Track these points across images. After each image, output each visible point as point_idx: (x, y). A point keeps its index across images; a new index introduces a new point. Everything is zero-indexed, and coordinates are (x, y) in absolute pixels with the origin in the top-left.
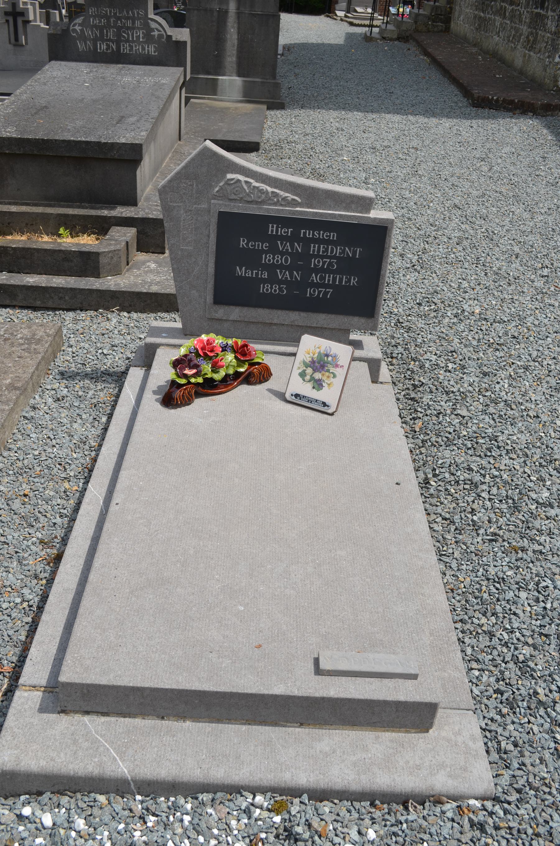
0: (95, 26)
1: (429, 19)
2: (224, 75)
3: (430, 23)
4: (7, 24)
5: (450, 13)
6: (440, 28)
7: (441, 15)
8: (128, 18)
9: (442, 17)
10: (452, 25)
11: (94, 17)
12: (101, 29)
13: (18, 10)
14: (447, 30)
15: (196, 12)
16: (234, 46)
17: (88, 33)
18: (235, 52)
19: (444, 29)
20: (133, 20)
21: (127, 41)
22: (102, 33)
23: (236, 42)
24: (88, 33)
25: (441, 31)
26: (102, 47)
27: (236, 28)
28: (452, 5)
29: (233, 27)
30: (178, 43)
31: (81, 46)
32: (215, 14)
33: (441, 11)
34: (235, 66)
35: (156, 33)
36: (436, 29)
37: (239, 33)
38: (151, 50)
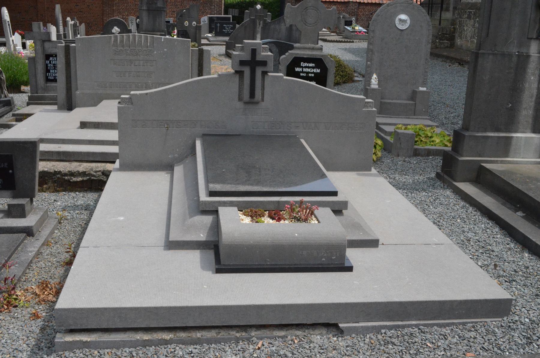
1: (436, 38)
2: (516, 132)
3: (437, 41)
4: (238, 76)
5: (454, 32)
6: (446, 45)
7: (447, 34)
9: (448, 36)
10: (458, 42)
13: (258, 58)
14: (452, 45)
15: (491, 57)
16: (532, 97)
18: (532, 104)
19: (449, 45)
23: (535, 92)
25: (447, 47)
27: (537, 76)
28: (455, 26)
29: (533, 74)
32: (515, 59)
33: (447, 31)
34: (530, 120)
36: (442, 46)
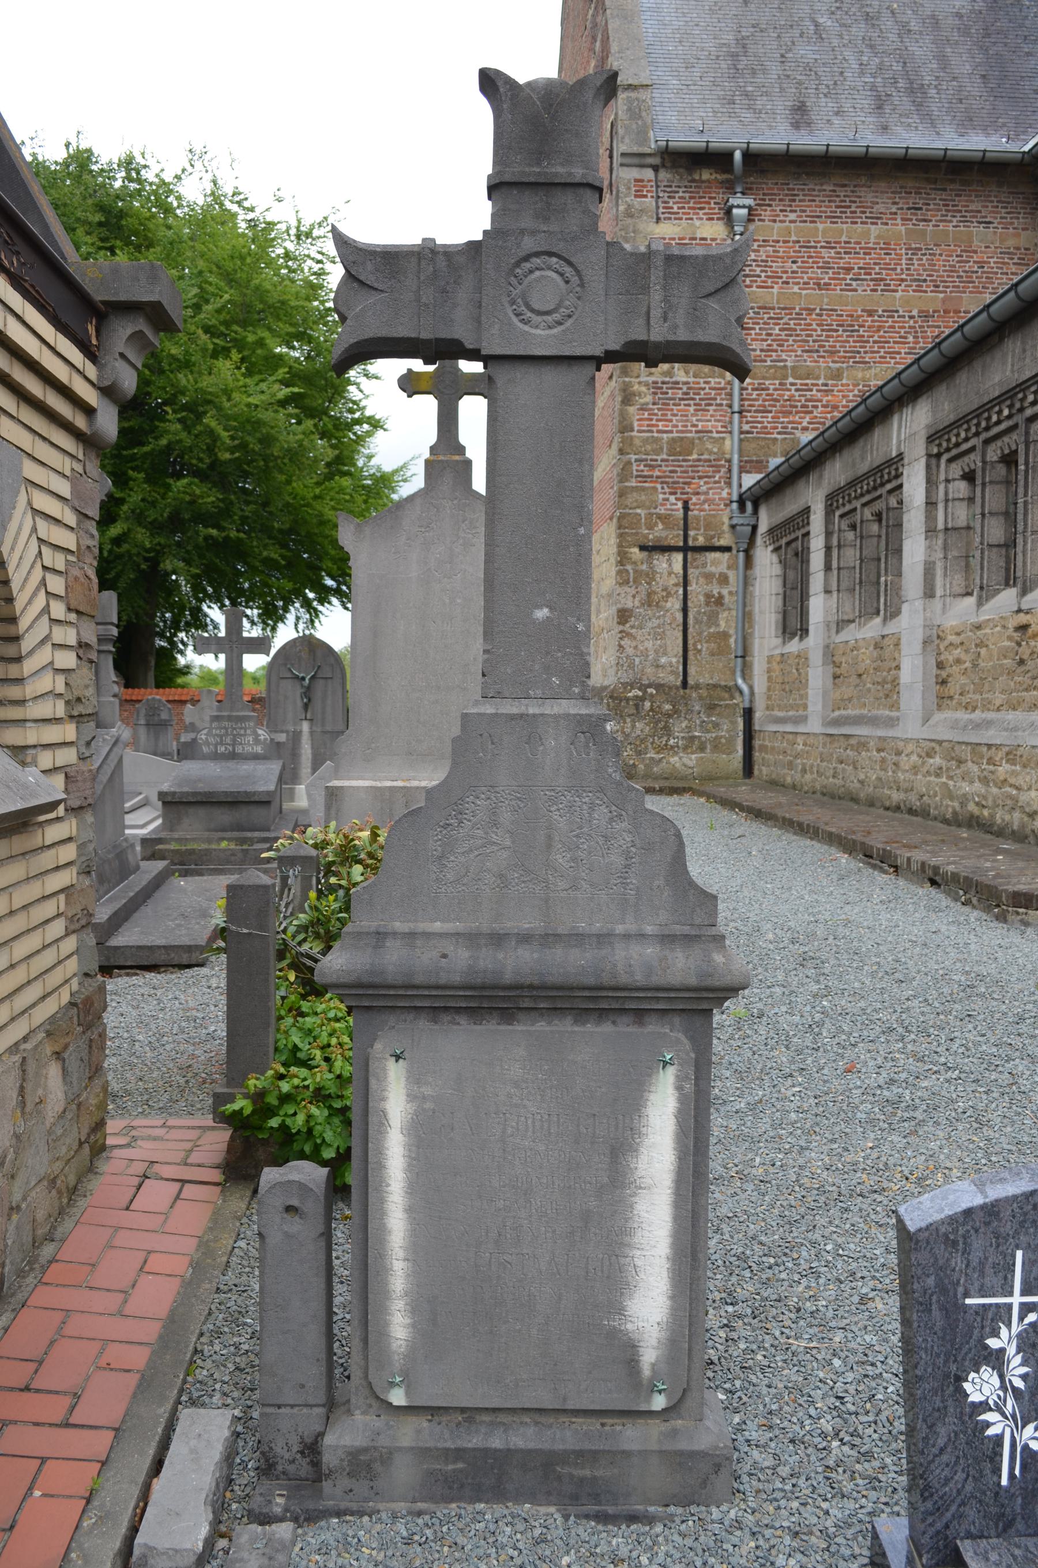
0: (217, 735)
8: (241, 728)
11: (216, 729)
12: (221, 737)
17: (211, 740)
18: (309, 765)
20: (245, 729)
21: (241, 744)
22: (221, 740)
23: (310, 756)
24: (211, 740)
26: (221, 749)
30: (278, 743)
31: (205, 749)
35: (262, 737)
37: (312, 748)
38: (259, 749)
